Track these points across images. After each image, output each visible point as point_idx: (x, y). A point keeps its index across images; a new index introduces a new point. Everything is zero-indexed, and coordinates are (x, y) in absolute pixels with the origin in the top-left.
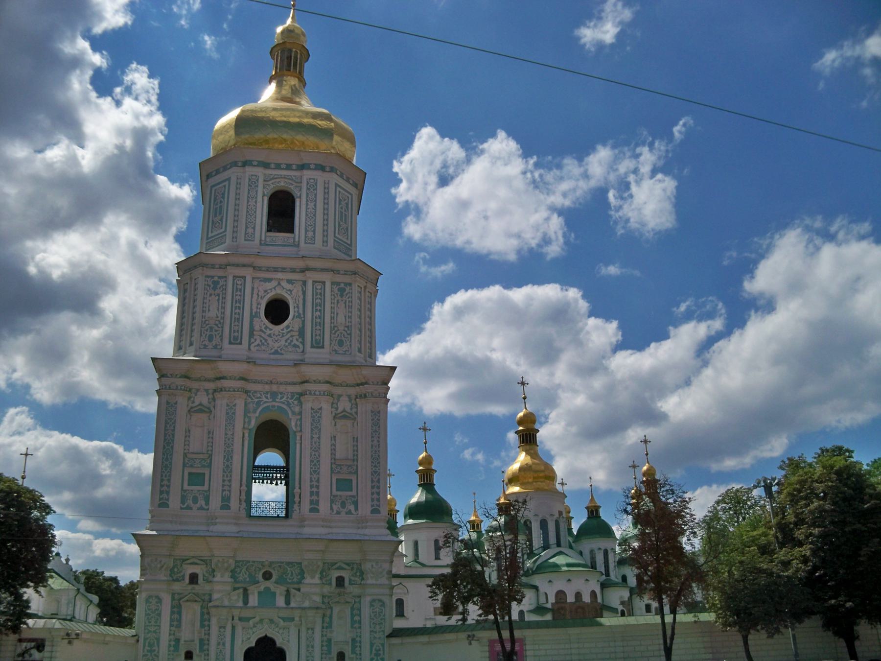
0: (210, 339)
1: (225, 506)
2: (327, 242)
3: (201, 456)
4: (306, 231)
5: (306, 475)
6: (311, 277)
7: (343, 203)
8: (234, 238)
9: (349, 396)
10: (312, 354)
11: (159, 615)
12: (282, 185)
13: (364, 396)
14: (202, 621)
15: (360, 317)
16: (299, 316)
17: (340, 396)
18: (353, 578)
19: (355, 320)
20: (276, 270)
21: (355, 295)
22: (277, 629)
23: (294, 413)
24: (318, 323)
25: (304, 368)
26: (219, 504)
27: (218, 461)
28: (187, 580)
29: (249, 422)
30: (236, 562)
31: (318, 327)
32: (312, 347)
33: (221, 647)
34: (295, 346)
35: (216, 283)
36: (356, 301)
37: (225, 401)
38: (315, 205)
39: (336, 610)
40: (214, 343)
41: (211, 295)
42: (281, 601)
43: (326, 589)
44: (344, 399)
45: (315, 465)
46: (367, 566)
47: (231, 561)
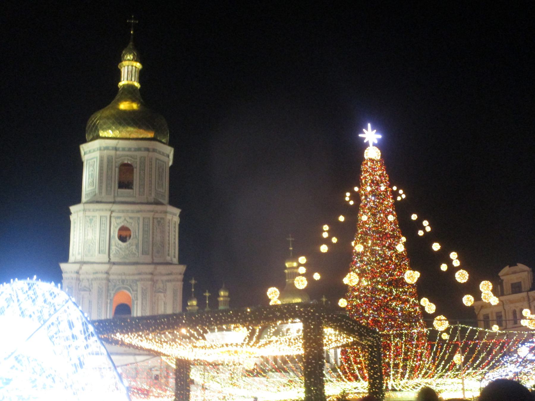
2: (151, 194)
9: (162, 281)
17: (157, 281)
29: (110, 296)
38: (144, 173)
41: (88, 227)
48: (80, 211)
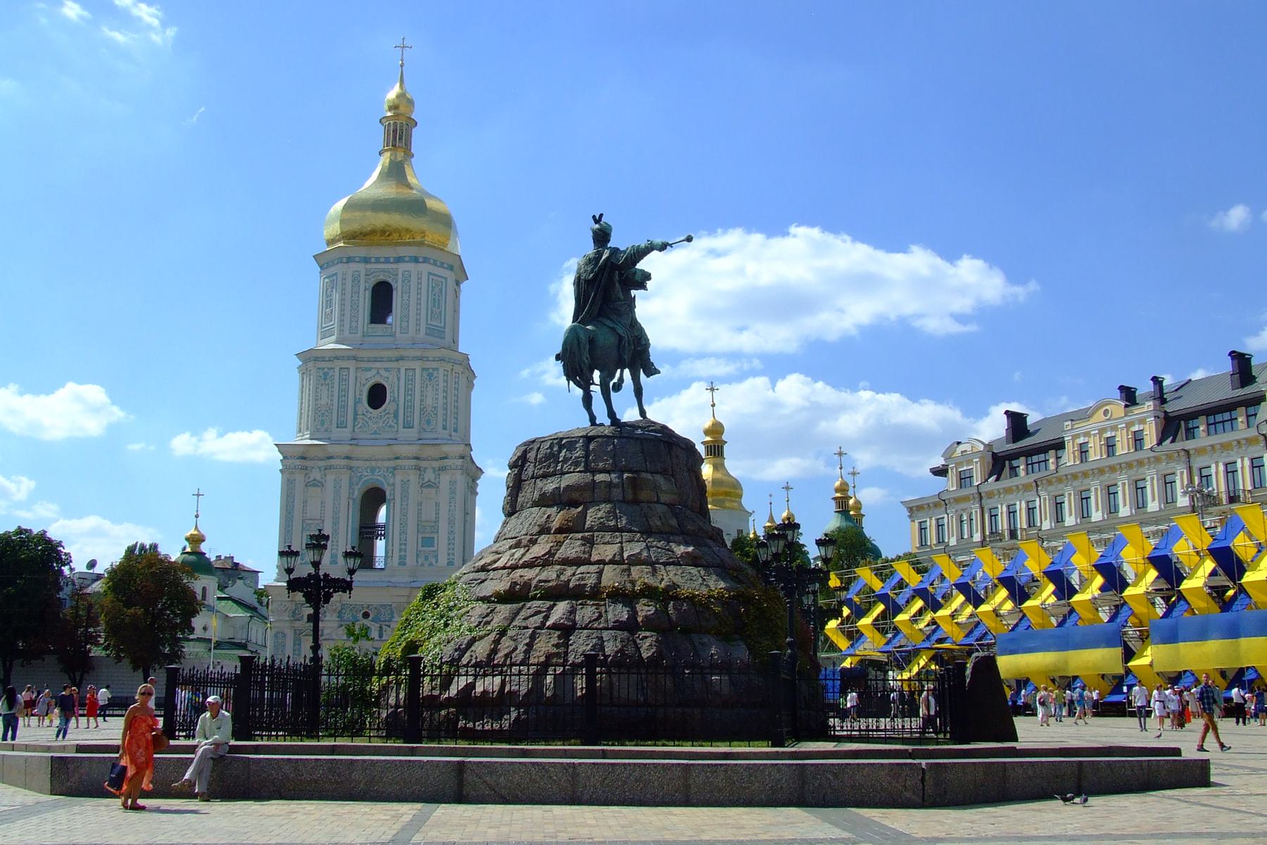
0: (322, 424)
6: (404, 365)
7: (437, 290)
8: (341, 331)
10: (405, 433)
12: (382, 278)
13: (442, 469)
21: (441, 376)
25: (396, 448)
35: (326, 374)
44: (430, 471)
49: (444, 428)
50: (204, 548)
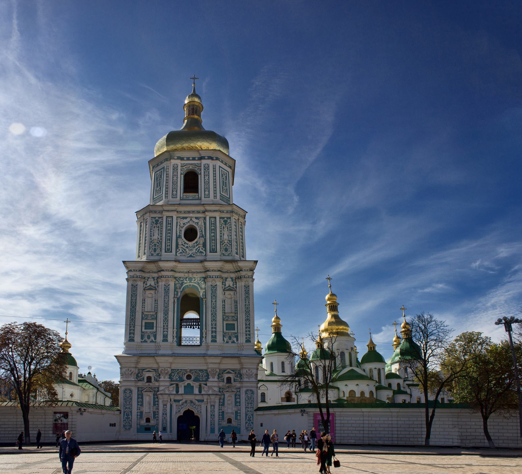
0: (155, 250)
1: (165, 340)
3: (152, 313)
4: (205, 191)
5: (209, 323)
9: (232, 278)
10: (210, 256)
11: (131, 399)
13: (240, 278)
14: (154, 402)
15: (236, 236)
16: (202, 236)
17: (226, 278)
18: (236, 378)
19: (234, 237)
20: (189, 212)
21: (233, 224)
22: (194, 406)
23: (201, 288)
24: (213, 239)
26: (162, 339)
27: (161, 315)
28: (145, 380)
29: (177, 294)
30: (172, 370)
31: (213, 242)
32: (210, 252)
33: (165, 416)
34: (201, 252)
35: (157, 221)
36: (233, 227)
37: (163, 283)
39: (227, 395)
40: (157, 252)
41: (154, 227)
42: (196, 391)
43: (221, 384)
45: (214, 316)
46: (244, 371)
47: (169, 369)
48: (146, 213)
49: (237, 253)
50: (70, 351)
